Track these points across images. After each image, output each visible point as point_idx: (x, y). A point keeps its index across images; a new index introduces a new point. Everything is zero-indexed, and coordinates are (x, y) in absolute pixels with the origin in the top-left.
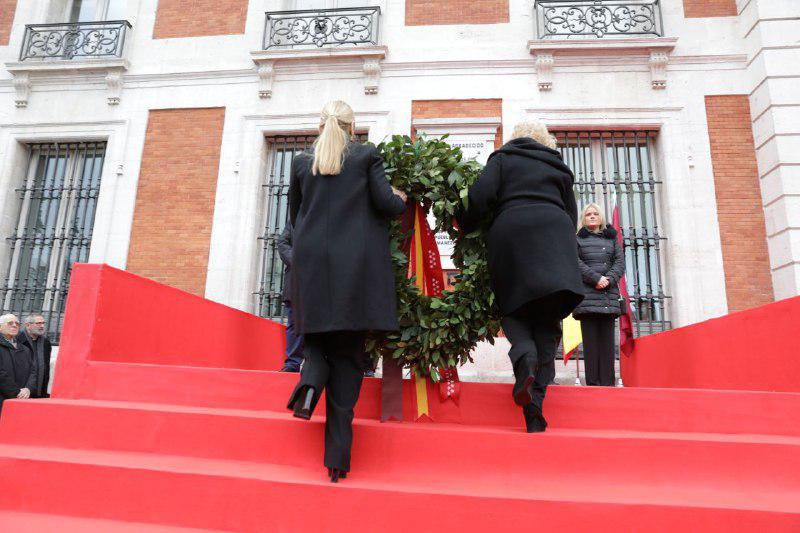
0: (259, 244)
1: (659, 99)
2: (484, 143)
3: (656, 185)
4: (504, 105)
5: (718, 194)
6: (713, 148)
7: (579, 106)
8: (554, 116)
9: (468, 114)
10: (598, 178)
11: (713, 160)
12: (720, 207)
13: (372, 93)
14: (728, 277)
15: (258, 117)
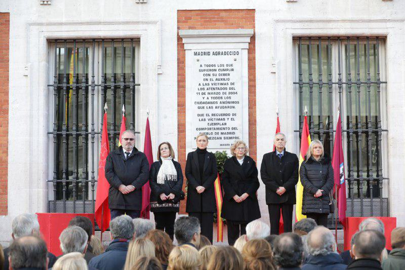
0: (48, 137)
2: (240, 51)
4: (257, 16)
7: (321, 17)
8: (298, 25)
13: (142, 3)
15: (41, 24)
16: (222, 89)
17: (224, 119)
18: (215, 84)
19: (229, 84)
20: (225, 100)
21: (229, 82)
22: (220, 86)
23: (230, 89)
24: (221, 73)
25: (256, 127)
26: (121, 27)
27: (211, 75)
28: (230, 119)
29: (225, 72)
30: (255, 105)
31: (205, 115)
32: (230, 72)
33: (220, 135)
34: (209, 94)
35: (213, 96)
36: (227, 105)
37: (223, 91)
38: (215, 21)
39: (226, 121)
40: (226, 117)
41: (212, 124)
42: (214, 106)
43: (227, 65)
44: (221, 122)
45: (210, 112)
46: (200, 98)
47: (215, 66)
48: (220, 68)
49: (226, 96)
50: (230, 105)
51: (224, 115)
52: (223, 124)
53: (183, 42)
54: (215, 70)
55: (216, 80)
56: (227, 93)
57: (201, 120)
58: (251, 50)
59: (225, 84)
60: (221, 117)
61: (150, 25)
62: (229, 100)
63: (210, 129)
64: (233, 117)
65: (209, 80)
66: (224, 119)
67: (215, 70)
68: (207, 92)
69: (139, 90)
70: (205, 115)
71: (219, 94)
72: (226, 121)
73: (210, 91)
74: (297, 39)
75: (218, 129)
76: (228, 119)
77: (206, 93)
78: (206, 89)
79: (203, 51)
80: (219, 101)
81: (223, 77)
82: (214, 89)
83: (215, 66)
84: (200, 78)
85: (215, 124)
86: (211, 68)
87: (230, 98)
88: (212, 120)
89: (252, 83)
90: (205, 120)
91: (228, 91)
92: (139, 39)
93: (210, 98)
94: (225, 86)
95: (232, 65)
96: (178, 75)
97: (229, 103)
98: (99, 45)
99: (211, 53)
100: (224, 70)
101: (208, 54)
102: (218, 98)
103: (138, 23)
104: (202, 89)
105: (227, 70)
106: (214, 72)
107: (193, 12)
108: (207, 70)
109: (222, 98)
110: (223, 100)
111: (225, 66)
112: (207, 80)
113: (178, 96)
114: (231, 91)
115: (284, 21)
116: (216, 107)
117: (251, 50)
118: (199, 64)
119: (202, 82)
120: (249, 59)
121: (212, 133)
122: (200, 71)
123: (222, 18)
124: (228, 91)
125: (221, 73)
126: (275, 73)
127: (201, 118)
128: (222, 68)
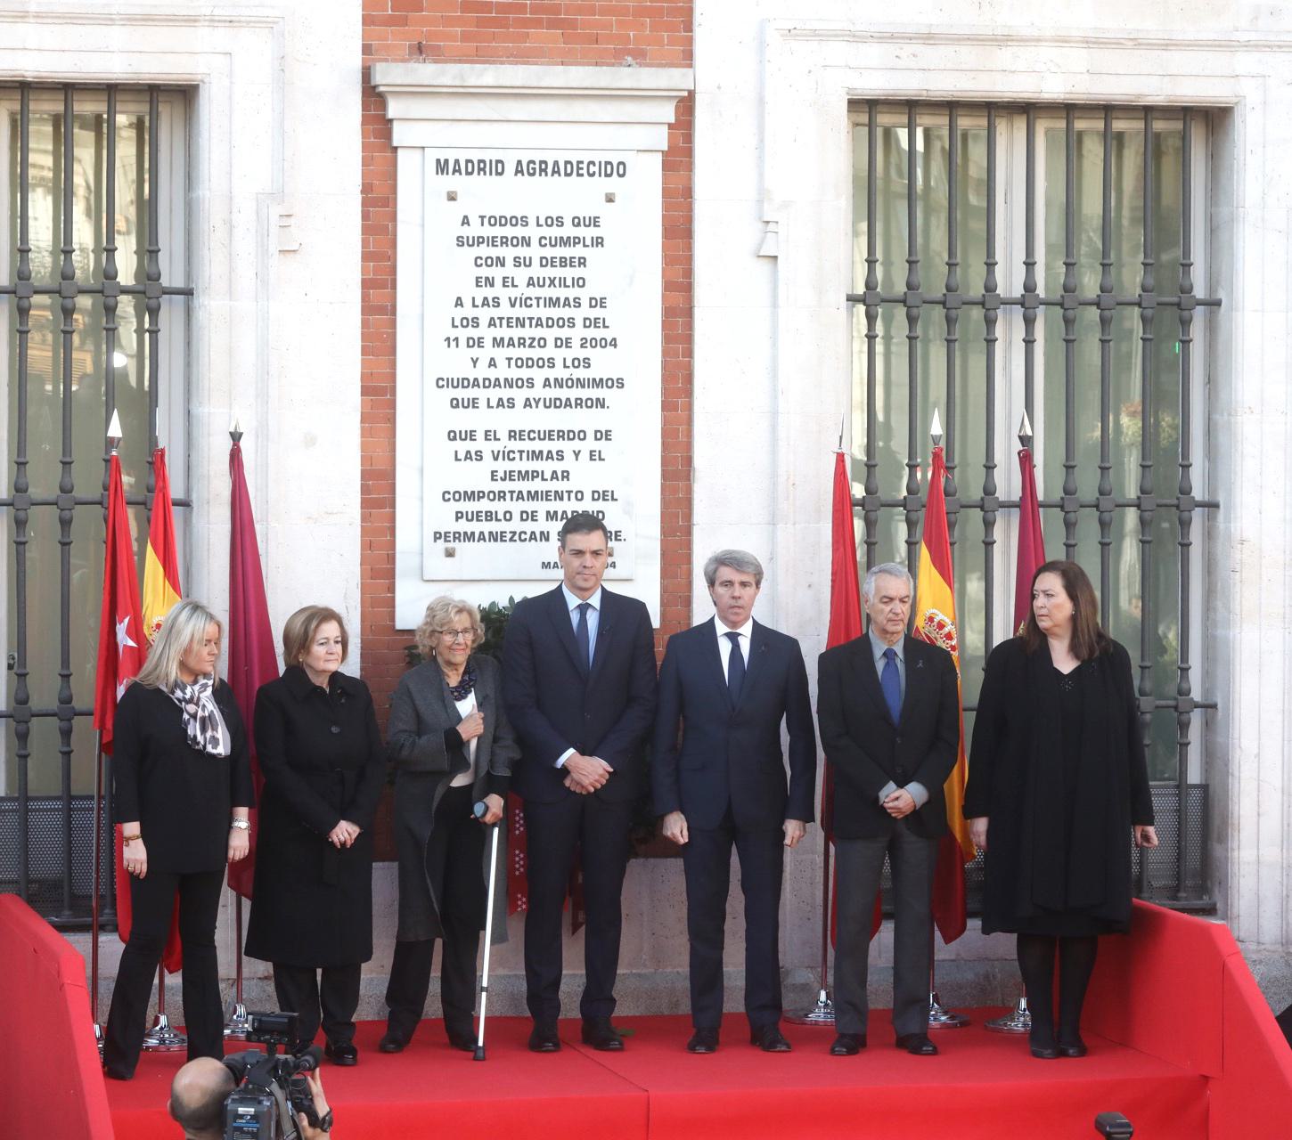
8: (874, 54)
10: (1010, 281)
16: (551, 323)
17: (561, 456)
18: (525, 301)
19: (585, 302)
22: (544, 312)
23: (589, 323)
24: (549, 252)
25: (689, 490)
26: (118, 36)
27: (509, 262)
28: (585, 456)
29: (567, 252)
31: (480, 435)
32: (589, 253)
33: (542, 525)
34: (498, 342)
35: (516, 352)
36: (575, 393)
37: (556, 332)
39: (568, 463)
40: (567, 446)
41: (509, 476)
42: (520, 395)
43: (577, 222)
44: (547, 467)
45: (503, 421)
46: (458, 363)
47: (524, 221)
50: (585, 393)
51: (561, 435)
52: (554, 476)
53: (391, 114)
54: (526, 242)
55: (531, 282)
56: (576, 343)
57: (461, 455)
59: (567, 303)
60: (545, 446)
62: (581, 373)
63: (501, 496)
64: (597, 446)
65: (498, 282)
66: (561, 456)
67: (526, 242)
68: (488, 334)
70: (480, 435)
71: (542, 343)
72: (568, 463)
73: (504, 332)
75: (534, 496)
76: (577, 454)
77: (488, 342)
78: (484, 322)
79: (475, 156)
80: (539, 375)
81: (558, 272)
82: (520, 323)
83: (524, 221)
84: (459, 272)
85: (524, 476)
86: (509, 231)
87: (587, 363)
88: (508, 455)
89: (678, 299)
90: (479, 456)
91: (577, 333)
93: (502, 363)
94: (565, 313)
95: (595, 222)
96: (366, 257)
97: (581, 383)
99: (510, 168)
100: (566, 242)
101: (498, 168)
102: (540, 363)
103: (191, 21)
105: (576, 241)
106: (522, 251)
108: (492, 242)
109: (551, 363)
110: (559, 372)
111: (568, 221)
112: (490, 282)
113: (365, 351)
114: (591, 333)
115: (816, 35)
116: (527, 403)
118: (458, 210)
119: (469, 292)
121: (508, 516)
122: (461, 242)
124: (577, 333)
125: (549, 252)
126: (776, 257)
127: (462, 447)
128: (555, 232)
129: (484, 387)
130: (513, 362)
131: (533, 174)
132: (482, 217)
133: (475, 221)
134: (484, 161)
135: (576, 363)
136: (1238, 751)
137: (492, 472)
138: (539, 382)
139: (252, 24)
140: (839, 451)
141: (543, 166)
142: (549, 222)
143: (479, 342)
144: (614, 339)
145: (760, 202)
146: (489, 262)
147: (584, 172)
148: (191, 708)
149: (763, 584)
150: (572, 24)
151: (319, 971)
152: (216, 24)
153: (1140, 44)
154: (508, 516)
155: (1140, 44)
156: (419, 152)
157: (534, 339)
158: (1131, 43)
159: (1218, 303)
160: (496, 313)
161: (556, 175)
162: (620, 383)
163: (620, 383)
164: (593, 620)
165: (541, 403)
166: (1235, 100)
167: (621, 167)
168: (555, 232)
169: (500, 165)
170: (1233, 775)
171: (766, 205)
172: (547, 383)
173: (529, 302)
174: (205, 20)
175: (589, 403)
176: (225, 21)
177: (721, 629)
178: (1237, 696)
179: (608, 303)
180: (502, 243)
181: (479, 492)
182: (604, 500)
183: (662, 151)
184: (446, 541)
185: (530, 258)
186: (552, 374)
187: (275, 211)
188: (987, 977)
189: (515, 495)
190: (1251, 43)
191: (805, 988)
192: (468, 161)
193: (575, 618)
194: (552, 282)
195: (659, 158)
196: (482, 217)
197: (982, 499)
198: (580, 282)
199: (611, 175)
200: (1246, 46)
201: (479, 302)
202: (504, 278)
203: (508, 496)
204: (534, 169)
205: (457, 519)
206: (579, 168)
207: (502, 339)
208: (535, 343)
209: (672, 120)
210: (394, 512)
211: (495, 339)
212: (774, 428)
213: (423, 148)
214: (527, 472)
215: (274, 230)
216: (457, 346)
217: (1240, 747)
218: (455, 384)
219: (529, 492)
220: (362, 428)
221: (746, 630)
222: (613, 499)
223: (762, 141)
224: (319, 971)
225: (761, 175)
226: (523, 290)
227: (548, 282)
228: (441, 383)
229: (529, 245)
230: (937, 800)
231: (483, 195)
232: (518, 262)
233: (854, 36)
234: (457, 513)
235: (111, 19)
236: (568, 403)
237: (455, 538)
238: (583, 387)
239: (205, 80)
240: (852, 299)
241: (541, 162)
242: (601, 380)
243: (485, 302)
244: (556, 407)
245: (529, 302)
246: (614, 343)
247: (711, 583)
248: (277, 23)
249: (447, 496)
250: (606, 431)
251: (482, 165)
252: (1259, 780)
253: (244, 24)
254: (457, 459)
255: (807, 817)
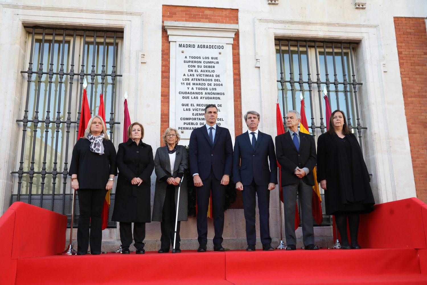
1: (360, 17)
2: (225, 45)
3: (357, 86)
4: (240, 14)
5: (405, 94)
6: (400, 58)
7: (300, 19)
8: (280, 26)
9: (211, 21)
11: (401, 67)
12: (406, 104)
14: (413, 161)
15: (16, 7)
16: (206, 80)
18: (200, 75)
19: (215, 76)
20: (210, 92)
21: (214, 74)
22: (205, 78)
23: (215, 80)
24: (206, 65)
26: (104, 16)
27: (196, 66)
30: (240, 98)
31: (190, 105)
32: (216, 65)
34: (194, 84)
35: (198, 86)
36: (212, 96)
37: (208, 82)
38: (200, 18)
41: (197, 114)
42: (199, 96)
43: (212, 58)
45: (195, 102)
46: (184, 88)
47: (200, 58)
48: (205, 60)
49: (211, 87)
53: (168, 33)
55: (201, 71)
56: (213, 85)
58: (236, 46)
61: (134, 16)
62: (214, 91)
63: (195, 119)
65: (194, 71)
68: (192, 82)
69: (120, 82)
70: (190, 105)
71: (205, 84)
73: (195, 82)
74: (280, 40)
77: (191, 84)
78: (190, 79)
79: (188, 44)
80: (204, 92)
81: (208, 69)
82: (199, 80)
83: (200, 58)
84: (185, 68)
86: (196, 60)
87: (215, 89)
88: (197, 110)
89: (237, 77)
90: (190, 110)
91: (213, 82)
92: (123, 29)
93: (195, 89)
94: (210, 78)
95: (217, 58)
96: (163, 66)
97: (214, 94)
98: (81, 39)
100: (210, 62)
101: (194, 46)
102: (204, 89)
103: (121, 13)
104: (186, 79)
105: (212, 62)
106: (199, 64)
107: (178, 9)
108: (192, 62)
109: (207, 89)
110: (209, 91)
111: (210, 58)
113: (162, 86)
115: (267, 21)
116: (201, 98)
117: (236, 46)
119: (187, 73)
120: (234, 55)
122: (185, 62)
123: (207, 15)
124: (213, 82)
125: (206, 65)
126: (259, 67)
127: (185, 108)
128: (207, 60)
129: (191, 94)
130: (197, 89)
131: (202, 48)
132: (190, 57)
133: (188, 57)
134: (190, 45)
135: (213, 89)
136: (380, 183)
137: (193, 113)
138: (204, 93)
139: (136, 15)
140: (277, 103)
141: (204, 46)
142: (206, 58)
143: (189, 84)
144: (222, 84)
145: (255, 56)
146: (192, 66)
147: (214, 47)
148: (92, 141)
149: (260, 120)
150: (211, 18)
151: (133, 224)
152: (128, 14)
153: (340, 25)
154: (197, 124)
155: (340, 25)
156: (175, 43)
157: (202, 84)
158: (337, 25)
159: (362, 84)
160: (193, 78)
161: (207, 48)
162: (224, 94)
163: (224, 94)
164: (214, 132)
165: (205, 98)
166: (362, 38)
167: (222, 47)
168: (207, 60)
169: (194, 46)
170: (379, 190)
171: (256, 56)
172: (206, 93)
173: (201, 75)
174: (125, 13)
175: (216, 98)
176: (130, 14)
177: (250, 132)
178: (378, 170)
179: (220, 76)
180: (195, 62)
181: (189, 118)
182: (220, 120)
183: (232, 44)
184: (181, 129)
185: (201, 66)
186: (207, 92)
187: (140, 54)
188: (323, 240)
189: (198, 119)
190: (365, 25)
191: (276, 243)
192: (186, 45)
193: (209, 131)
194: (207, 71)
195: (231, 46)
196: (190, 57)
197: (311, 126)
198: (213, 71)
199: (220, 48)
200: (363, 26)
201: (189, 75)
202: (195, 70)
203: (197, 119)
204: (202, 47)
205: (184, 124)
206: (212, 47)
207: (195, 83)
208: (203, 85)
209: (234, 36)
210: (169, 124)
211: (193, 83)
212: (261, 105)
213: (176, 42)
214: (201, 114)
215: (140, 58)
216: (184, 85)
217: (380, 182)
218: (184, 93)
219: (202, 118)
220: (161, 104)
221: (256, 132)
222: (223, 120)
223: (255, 43)
224: (133, 224)
225: (255, 50)
226: (199, 73)
227: (206, 71)
228: (180, 93)
229: (201, 63)
230: (311, 173)
231: (190, 52)
232: (198, 66)
233: (275, 21)
234: (184, 123)
235: (103, 12)
236: (211, 98)
237: (184, 129)
238: (215, 94)
239: (125, 26)
240: (278, 81)
241: (204, 45)
242: (219, 93)
243: (191, 75)
244: (208, 99)
245: (201, 75)
246: (222, 85)
247: (246, 120)
248: (141, 14)
249: (182, 119)
250: (221, 105)
251: (190, 46)
252: (386, 191)
253: (134, 15)
254: (184, 110)
255: (276, 183)
